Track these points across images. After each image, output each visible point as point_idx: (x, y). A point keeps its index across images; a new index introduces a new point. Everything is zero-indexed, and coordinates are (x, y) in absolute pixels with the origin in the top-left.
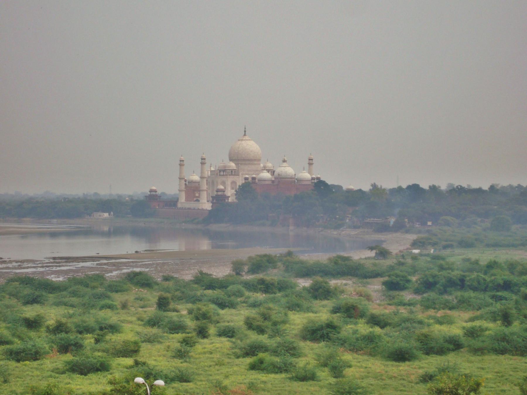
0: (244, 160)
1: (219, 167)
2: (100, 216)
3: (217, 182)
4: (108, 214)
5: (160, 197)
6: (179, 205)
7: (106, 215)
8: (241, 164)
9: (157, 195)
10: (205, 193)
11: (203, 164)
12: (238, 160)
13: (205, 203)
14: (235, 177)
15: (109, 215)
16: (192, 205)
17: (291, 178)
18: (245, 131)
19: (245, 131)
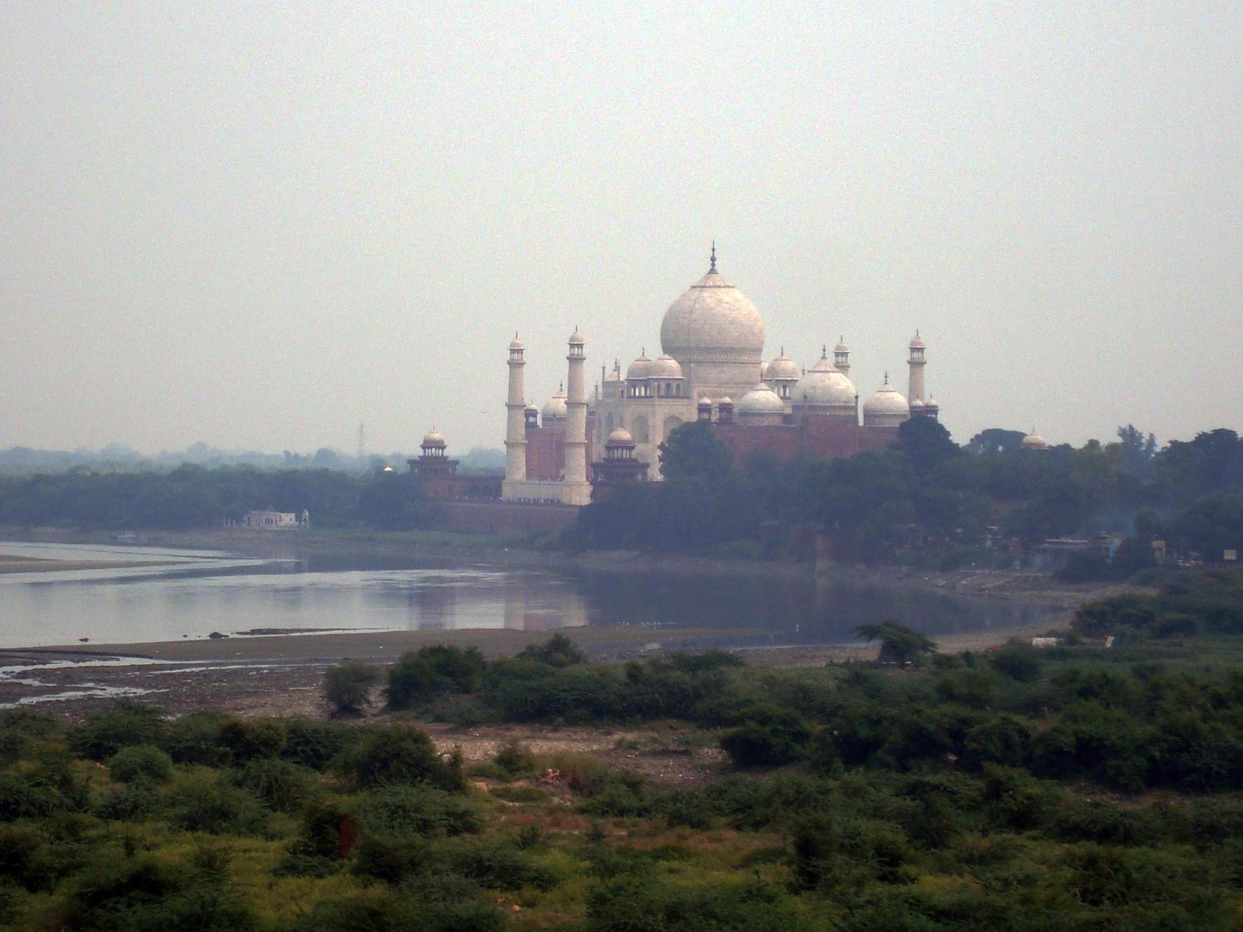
0: (708, 350)
1: (630, 372)
2: (269, 521)
3: (622, 420)
4: (293, 516)
5: (456, 462)
6: (507, 492)
7: (288, 519)
8: (699, 363)
9: (444, 459)
10: (583, 451)
11: (575, 361)
12: (689, 350)
13: (579, 485)
14: (679, 402)
15: (298, 518)
16: (542, 491)
17: (845, 408)
18: (713, 259)
19: (713, 259)
